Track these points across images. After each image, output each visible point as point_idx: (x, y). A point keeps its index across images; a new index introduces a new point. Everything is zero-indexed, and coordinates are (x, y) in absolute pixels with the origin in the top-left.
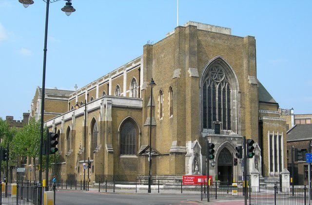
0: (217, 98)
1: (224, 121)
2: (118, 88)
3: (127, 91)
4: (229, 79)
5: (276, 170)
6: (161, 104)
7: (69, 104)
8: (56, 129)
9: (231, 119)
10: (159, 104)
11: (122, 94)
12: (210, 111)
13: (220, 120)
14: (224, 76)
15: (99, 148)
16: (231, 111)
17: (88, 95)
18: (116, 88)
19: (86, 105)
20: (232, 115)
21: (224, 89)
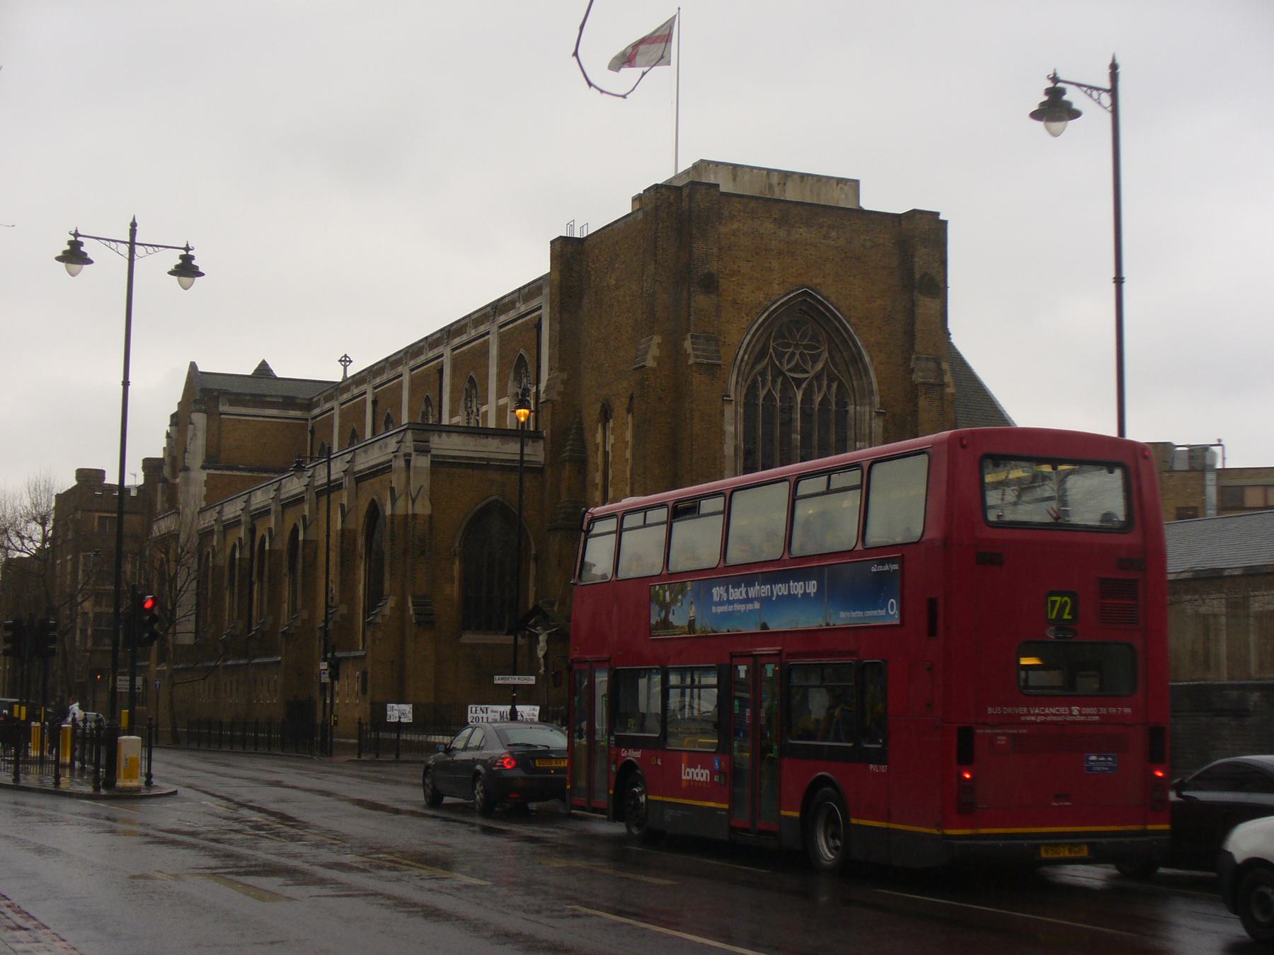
2: (472, 389)
3: (502, 401)
6: (606, 454)
7: (312, 432)
8: (252, 531)
10: (600, 453)
11: (484, 409)
14: (826, 355)
15: (387, 611)
17: (375, 403)
18: (467, 385)
19: (329, 461)
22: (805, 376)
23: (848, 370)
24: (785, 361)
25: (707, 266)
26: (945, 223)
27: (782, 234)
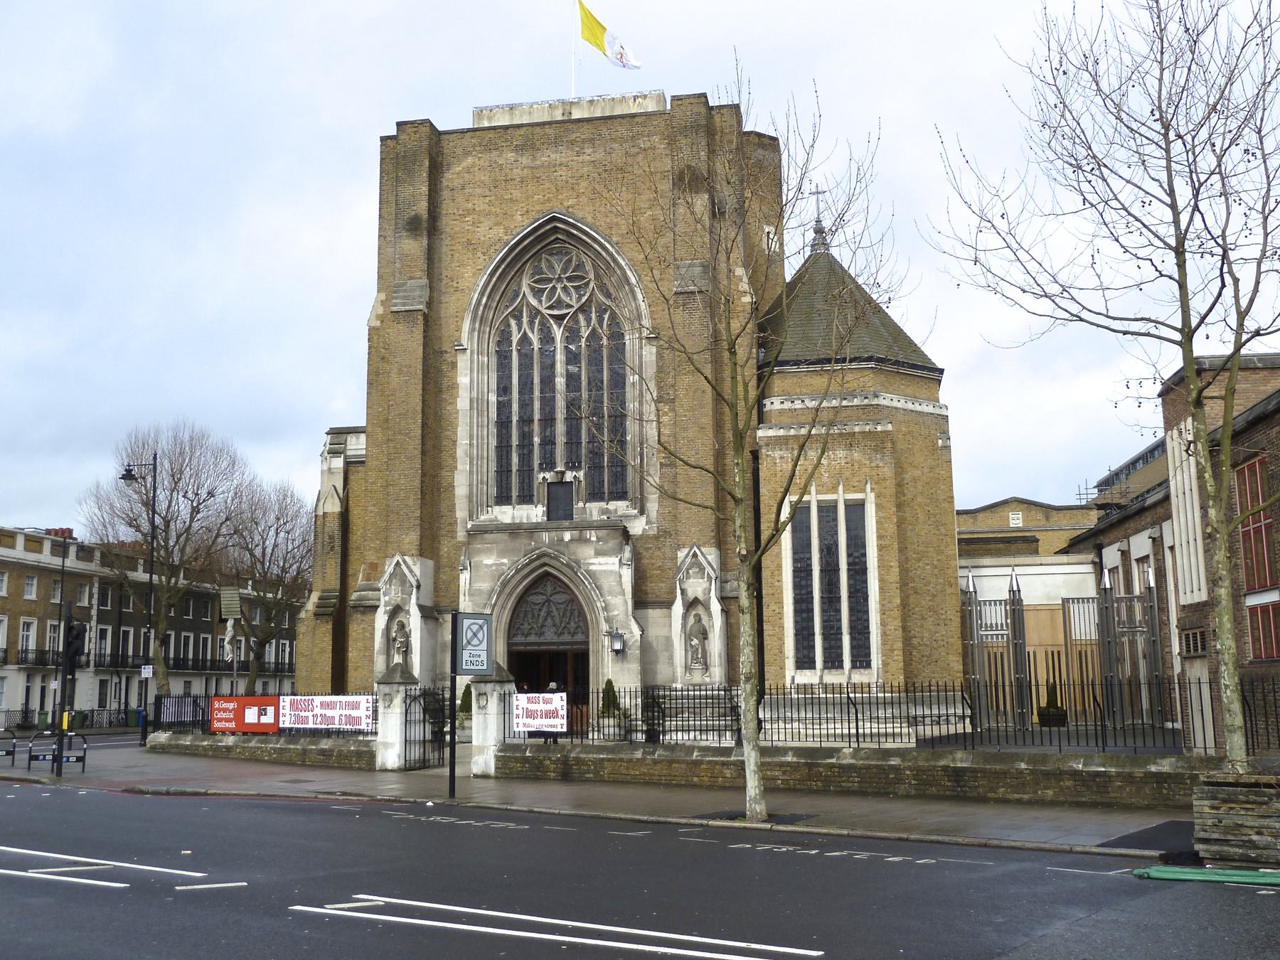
1: (596, 468)
12: (526, 438)
22: (567, 311)
25: (415, 208)
27: (525, 160)
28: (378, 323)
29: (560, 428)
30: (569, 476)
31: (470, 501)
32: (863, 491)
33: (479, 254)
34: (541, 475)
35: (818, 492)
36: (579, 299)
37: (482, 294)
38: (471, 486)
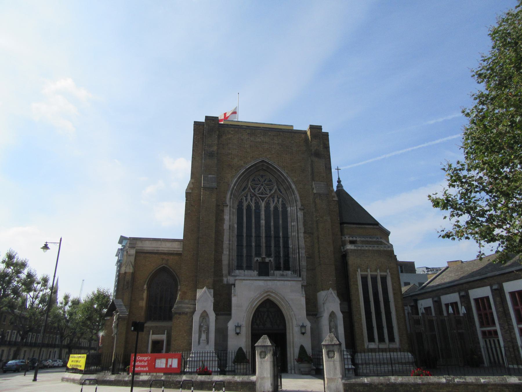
0: (263, 222)
1: (277, 257)
4: (284, 192)
5: (381, 339)
9: (291, 255)
13: (269, 255)
14: (276, 187)
16: (290, 242)
20: (291, 246)
21: (276, 208)
22: (266, 196)
23: (286, 193)
24: (257, 190)
26: (327, 135)
28: (190, 191)
29: (263, 240)
30: (267, 260)
31: (229, 267)
32: (386, 272)
33: (234, 170)
34: (256, 259)
35: (371, 271)
36: (270, 192)
37: (235, 185)
38: (229, 260)
